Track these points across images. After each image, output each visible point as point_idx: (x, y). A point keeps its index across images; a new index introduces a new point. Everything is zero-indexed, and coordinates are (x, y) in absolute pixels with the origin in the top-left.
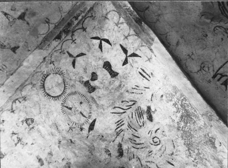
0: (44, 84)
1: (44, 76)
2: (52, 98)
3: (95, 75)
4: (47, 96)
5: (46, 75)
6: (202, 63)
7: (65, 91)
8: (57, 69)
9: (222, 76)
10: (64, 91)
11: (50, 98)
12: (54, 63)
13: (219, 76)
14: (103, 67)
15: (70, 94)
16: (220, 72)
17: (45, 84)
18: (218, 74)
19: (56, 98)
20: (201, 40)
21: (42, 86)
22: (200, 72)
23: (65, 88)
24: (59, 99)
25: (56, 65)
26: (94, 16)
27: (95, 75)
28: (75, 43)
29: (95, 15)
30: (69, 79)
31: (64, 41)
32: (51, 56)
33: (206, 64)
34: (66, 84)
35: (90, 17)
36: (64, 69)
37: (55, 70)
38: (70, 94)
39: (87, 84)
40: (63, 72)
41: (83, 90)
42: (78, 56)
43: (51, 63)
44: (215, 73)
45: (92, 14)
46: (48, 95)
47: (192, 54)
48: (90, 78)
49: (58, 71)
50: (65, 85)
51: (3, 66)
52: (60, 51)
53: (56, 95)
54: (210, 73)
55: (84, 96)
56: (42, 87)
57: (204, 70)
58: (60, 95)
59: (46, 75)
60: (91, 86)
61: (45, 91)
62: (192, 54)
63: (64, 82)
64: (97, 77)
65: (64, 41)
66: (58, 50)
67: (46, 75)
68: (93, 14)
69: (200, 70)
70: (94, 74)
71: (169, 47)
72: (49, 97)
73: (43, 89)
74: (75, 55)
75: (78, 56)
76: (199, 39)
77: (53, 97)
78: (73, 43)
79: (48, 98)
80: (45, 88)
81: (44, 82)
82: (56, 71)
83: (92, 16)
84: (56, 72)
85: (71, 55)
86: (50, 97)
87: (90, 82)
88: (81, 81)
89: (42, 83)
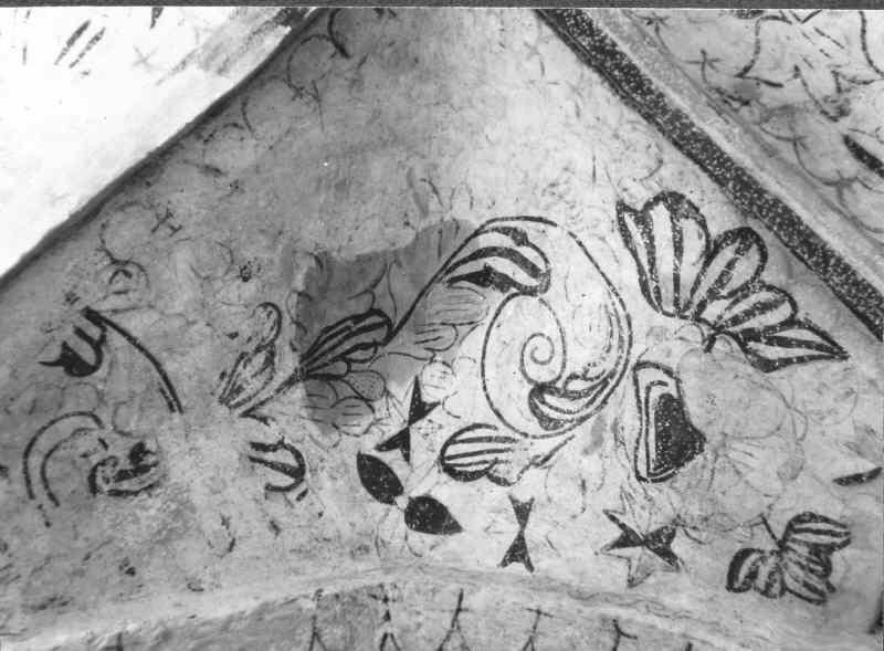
6: (141, 268)
9: (98, 346)
13: (94, 332)
16: (115, 339)
18: (104, 330)
20: (228, 256)
22: (107, 262)
33: (138, 282)
44: (107, 315)
47: (172, 228)
54: (105, 298)
57: (116, 274)
62: (172, 228)
69: (114, 262)
71: (199, 137)
76: (231, 252)
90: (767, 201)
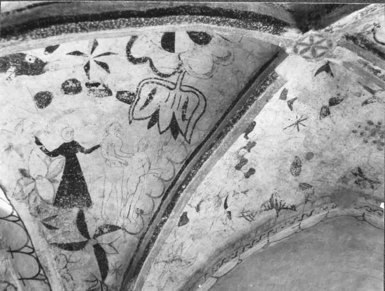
26: (373, 27)
29: (370, 25)
35: (374, 34)
45: (369, 33)
68: (369, 29)
83: (373, 30)
90: (123, 25)
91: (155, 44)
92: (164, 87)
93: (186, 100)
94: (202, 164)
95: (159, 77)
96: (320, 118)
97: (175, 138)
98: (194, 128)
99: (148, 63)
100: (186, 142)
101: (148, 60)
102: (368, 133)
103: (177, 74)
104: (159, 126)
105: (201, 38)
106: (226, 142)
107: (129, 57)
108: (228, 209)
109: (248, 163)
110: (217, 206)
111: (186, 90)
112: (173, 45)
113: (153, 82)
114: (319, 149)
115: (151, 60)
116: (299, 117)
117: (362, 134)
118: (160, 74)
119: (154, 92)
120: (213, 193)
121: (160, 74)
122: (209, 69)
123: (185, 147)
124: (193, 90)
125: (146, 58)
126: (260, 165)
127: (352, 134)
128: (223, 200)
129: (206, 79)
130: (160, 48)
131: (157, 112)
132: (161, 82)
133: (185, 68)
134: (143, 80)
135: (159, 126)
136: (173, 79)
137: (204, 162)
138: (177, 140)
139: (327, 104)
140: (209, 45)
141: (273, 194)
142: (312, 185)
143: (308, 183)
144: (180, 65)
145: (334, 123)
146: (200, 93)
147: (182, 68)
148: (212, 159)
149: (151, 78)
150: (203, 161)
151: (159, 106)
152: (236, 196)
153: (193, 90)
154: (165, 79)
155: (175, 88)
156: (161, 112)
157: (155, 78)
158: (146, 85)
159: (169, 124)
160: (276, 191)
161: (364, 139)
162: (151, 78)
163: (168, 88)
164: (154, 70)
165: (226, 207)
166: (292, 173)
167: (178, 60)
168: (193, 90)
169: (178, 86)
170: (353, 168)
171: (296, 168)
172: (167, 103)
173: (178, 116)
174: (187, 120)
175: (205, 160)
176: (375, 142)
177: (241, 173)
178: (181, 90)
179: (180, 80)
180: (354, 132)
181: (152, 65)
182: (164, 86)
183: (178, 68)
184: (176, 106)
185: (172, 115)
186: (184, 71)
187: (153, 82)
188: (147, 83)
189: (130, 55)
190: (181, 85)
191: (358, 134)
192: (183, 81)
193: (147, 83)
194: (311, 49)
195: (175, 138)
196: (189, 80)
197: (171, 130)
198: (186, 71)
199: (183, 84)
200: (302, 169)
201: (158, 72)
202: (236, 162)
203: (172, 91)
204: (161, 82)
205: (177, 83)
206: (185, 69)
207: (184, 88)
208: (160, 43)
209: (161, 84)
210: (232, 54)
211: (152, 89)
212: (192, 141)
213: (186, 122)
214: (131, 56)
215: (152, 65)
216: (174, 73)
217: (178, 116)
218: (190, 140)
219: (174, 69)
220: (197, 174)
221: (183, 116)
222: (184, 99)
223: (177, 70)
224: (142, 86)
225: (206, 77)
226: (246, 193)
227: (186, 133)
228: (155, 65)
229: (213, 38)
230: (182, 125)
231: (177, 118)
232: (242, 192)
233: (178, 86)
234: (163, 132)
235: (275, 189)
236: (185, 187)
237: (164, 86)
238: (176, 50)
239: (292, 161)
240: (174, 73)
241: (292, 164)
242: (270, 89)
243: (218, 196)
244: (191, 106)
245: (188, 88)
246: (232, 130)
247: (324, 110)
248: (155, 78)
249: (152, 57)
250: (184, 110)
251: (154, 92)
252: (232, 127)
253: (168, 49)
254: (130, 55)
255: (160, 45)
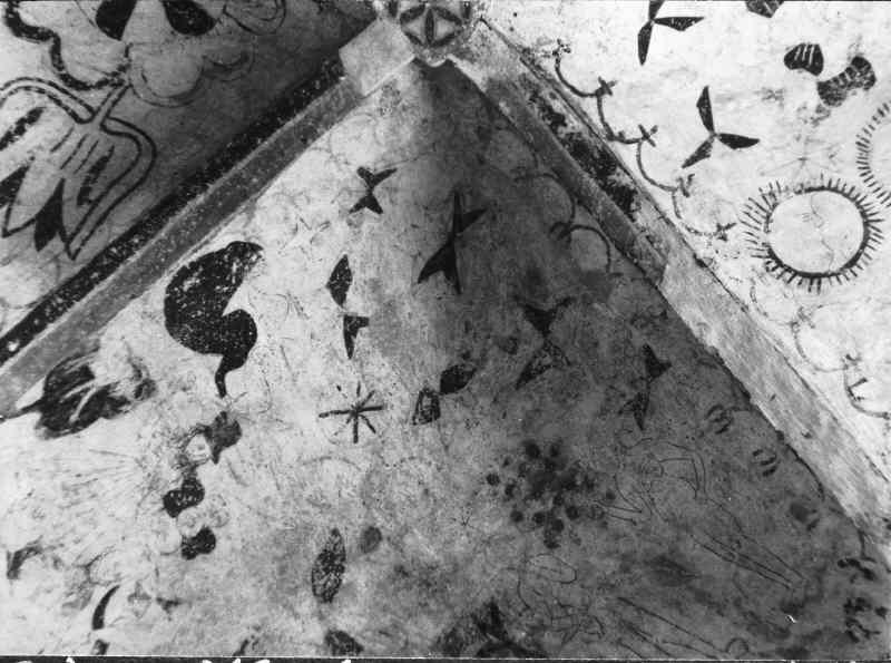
0: (805, 275)
1: (774, 269)
2: (867, 250)
3: (798, 53)
4: (855, 268)
5: (767, 260)
7: (847, 191)
8: (753, 213)
10: (847, 196)
11: (867, 255)
12: (724, 225)
14: (769, 16)
15: (865, 169)
17: (807, 270)
19: (873, 231)
21: (811, 283)
23: (835, 190)
24: (878, 221)
25: (734, 218)
26: (556, 46)
27: (798, 53)
28: (654, 130)
30: (801, 167)
31: (643, 172)
32: (696, 232)
34: (818, 184)
35: (558, 61)
36: (754, 185)
37: (752, 222)
38: (865, 169)
39: (830, 93)
40: (766, 190)
41: (857, 104)
42: (708, 123)
43: (724, 238)
46: (853, 262)
48: (807, 74)
49: (760, 211)
50: (822, 188)
51: (713, 417)
52: (679, 194)
53: (860, 229)
55: (882, 108)
56: (815, 285)
58: (863, 214)
59: (767, 260)
60: (842, 75)
61: (833, 274)
63: (810, 190)
64: (810, 46)
65: (643, 172)
66: (675, 203)
67: (769, 262)
68: (550, 48)
70: (796, 58)
72: (859, 262)
73: (824, 280)
74: (704, 134)
75: (708, 123)
77: (864, 245)
78: (651, 137)
79: (866, 264)
80: (822, 271)
81: (796, 273)
82: (759, 218)
83: (555, 53)
84: (763, 221)
85: (702, 152)
86: (863, 256)
87: (825, 76)
88: (816, 116)
89: (800, 283)
91: (83, 12)
92: (64, 112)
93: (107, 154)
94: (90, 287)
95: (60, 83)
96: (414, 418)
97: (39, 246)
98: (100, 222)
99: (46, 47)
100: (65, 257)
101: (52, 39)
102: (524, 486)
103: (108, 89)
104: (9, 211)
105: (191, 22)
106: (175, 232)
107: (11, 16)
108: (102, 634)
109: (204, 505)
110: (71, 605)
111: (115, 129)
112: (124, 23)
113: (41, 91)
114: (397, 523)
115: (58, 41)
116: (364, 392)
117: (509, 490)
118: (65, 78)
119: (34, 116)
120: (79, 548)
121: (65, 78)
122: (185, 86)
123: (58, 267)
124: (135, 133)
125: (50, 31)
126: (234, 528)
127: (486, 489)
128: (99, 593)
129: (173, 107)
130: (90, 21)
131: (20, 175)
132: (60, 96)
133: (132, 77)
134: (21, 79)
135: (9, 211)
136: (94, 98)
137: (97, 282)
138: (44, 251)
139: (435, 385)
140: (204, 37)
141: (246, 642)
142: (360, 641)
143: (352, 635)
144: (123, 69)
145: (447, 447)
146: (148, 138)
147: (124, 76)
148: (119, 282)
149: (40, 80)
150: (96, 275)
151: (33, 159)
152: (138, 605)
153: (132, 131)
154: (75, 93)
155: (90, 120)
156: (29, 176)
157: (51, 84)
158: (22, 92)
159: (38, 209)
160: (257, 635)
161: (515, 506)
162: (40, 80)
163: (74, 116)
164: (56, 63)
165: (98, 622)
166: (314, 590)
167: (122, 56)
168: (135, 133)
169: (99, 118)
170: (479, 606)
171: (327, 571)
172: (57, 154)
173: (70, 192)
174: (90, 202)
175: (103, 277)
176: (539, 518)
177: (177, 530)
178: (103, 127)
179: (109, 104)
180: (492, 480)
181: (56, 51)
182: (66, 108)
183: (114, 74)
184: (74, 164)
185: (54, 188)
186: (127, 84)
187: (41, 91)
188: (27, 88)
189: (15, 9)
190: (107, 116)
191: (501, 489)
192: (116, 109)
193: (27, 88)
194: (425, 14)
195: (39, 246)
196: (131, 108)
197: (38, 228)
198: (131, 86)
199: (112, 115)
200: (344, 581)
201: (64, 72)
202: (172, 479)
203: (78, 127)
204: (60, 96)
205: (99, 109)
206: (130, 79)
207: (112, 125)
208: (95, 13)
209: (58, 103)
210: (251, 58)
211: (31, 107)
212: (79, 258)
213: (86, 207)
214: (17, 15)
215: (56, 51)
216: (100, 85)
217: (70, 192)
218: (78, 251)
219: (107, 74)
220: (64, 319)
221: (83, 196)
222: (102, 150)
223: (109, 78)
224: (11, 93)
225: (175, 104)
226: (172, 608)
227: (74, 235)
228: (65, 54)
229: (217, 25)
230: (71, 215)
231: (65, 196)
232: (159, 600)
233: (99, 118)
234: (17, 230)
235: (258, 629)
236: (17, 351)
237: (66, 108)
238: (124, 37)
239: (322, 546)
240: (100, 85)
241: (320, 556)
242: (318, 107)
243: (87, 567)
244: (111, 171)
245: (120, 125)
246: (201, 199)
247: (427, 401)
248: (51, 84)
249: (63, 33)
250: (92, 176)
251: (34, 116)
252: (205, 188)
253: (108, 30)
254: (15, 9)
255: (92, 15)
